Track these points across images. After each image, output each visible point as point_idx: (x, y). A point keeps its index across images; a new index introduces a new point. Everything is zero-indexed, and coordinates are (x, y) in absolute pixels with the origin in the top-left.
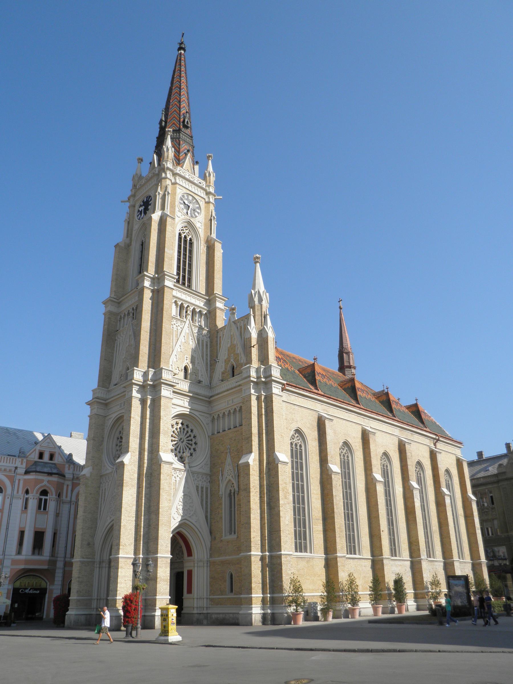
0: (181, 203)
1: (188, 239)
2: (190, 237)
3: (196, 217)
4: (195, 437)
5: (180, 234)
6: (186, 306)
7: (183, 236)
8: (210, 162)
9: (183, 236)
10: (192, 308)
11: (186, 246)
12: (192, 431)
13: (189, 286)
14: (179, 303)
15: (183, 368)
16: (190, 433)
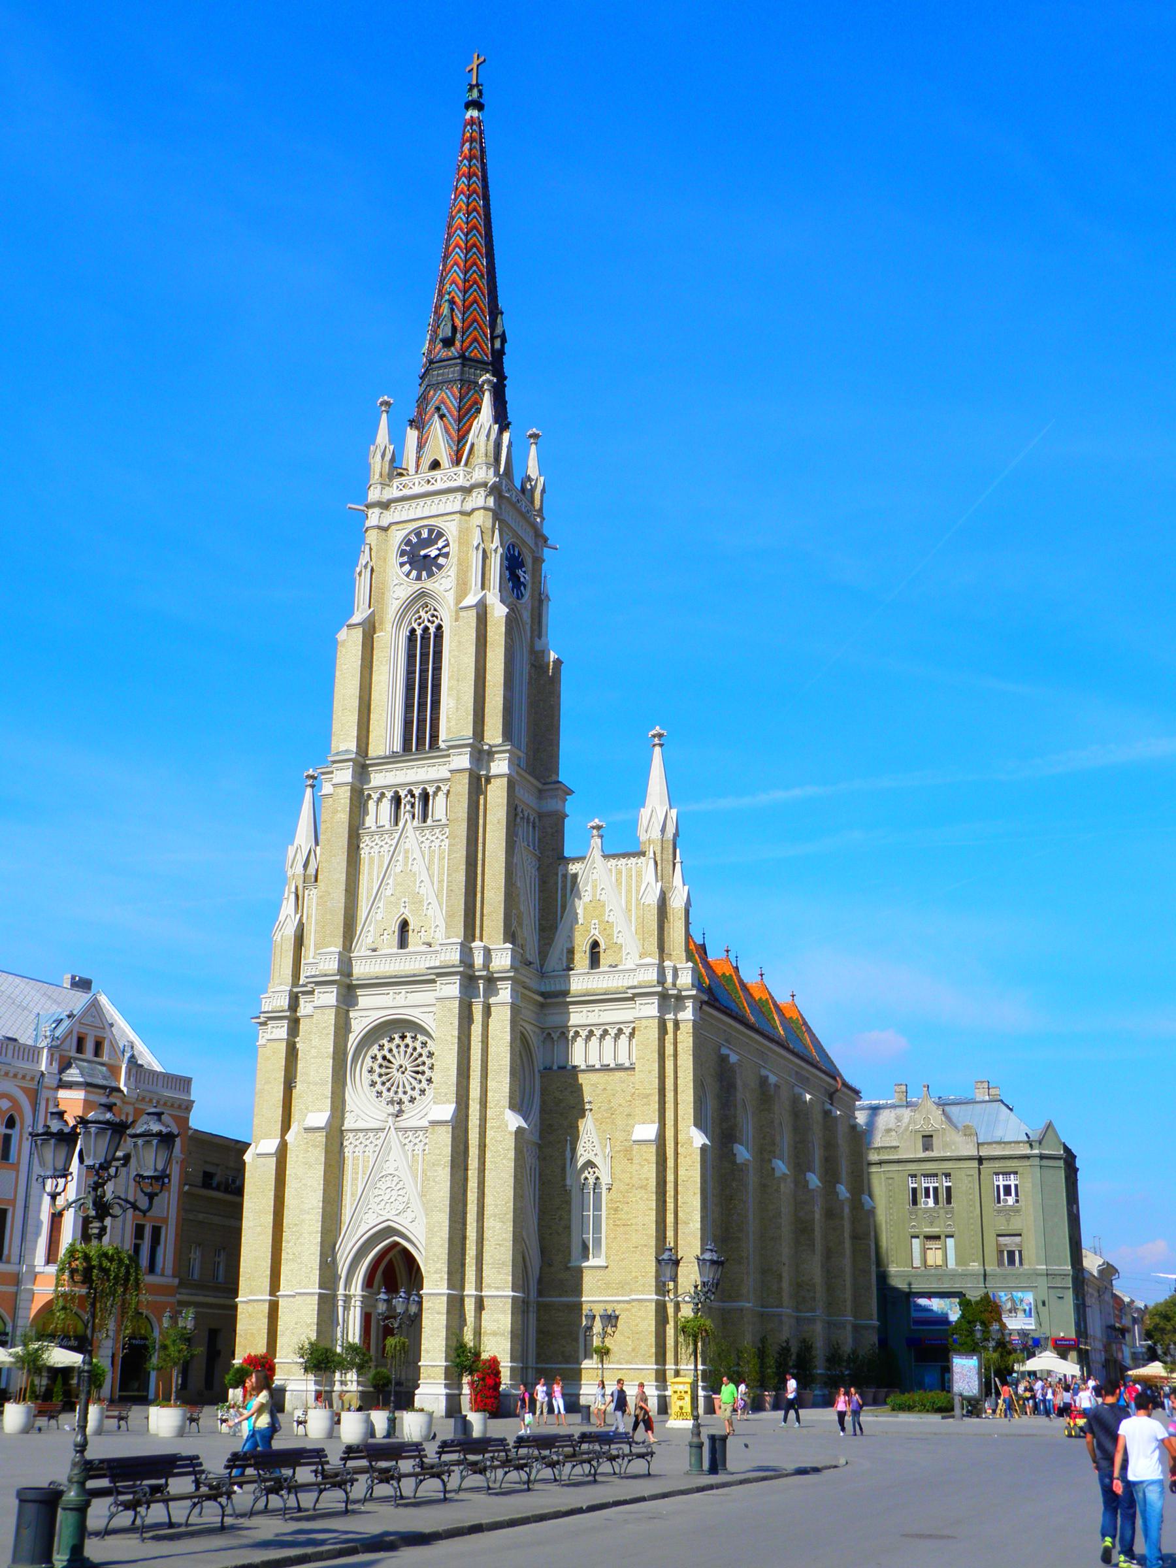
0: (402, 565)
1: (432, 630)
2: (437, 622)
3: (440, 567)
4: (430, 1055)
5: (413, 631)
6: (402, 793)
7: (419, 632)
8: (487, 394)
9: (419, 632)
10: (417, 792)
11: (424, 651)
12: (424, 1044)
13: (435, 737)
14: (389, 795)
15: (395, 927)
16: (419, 1050)
